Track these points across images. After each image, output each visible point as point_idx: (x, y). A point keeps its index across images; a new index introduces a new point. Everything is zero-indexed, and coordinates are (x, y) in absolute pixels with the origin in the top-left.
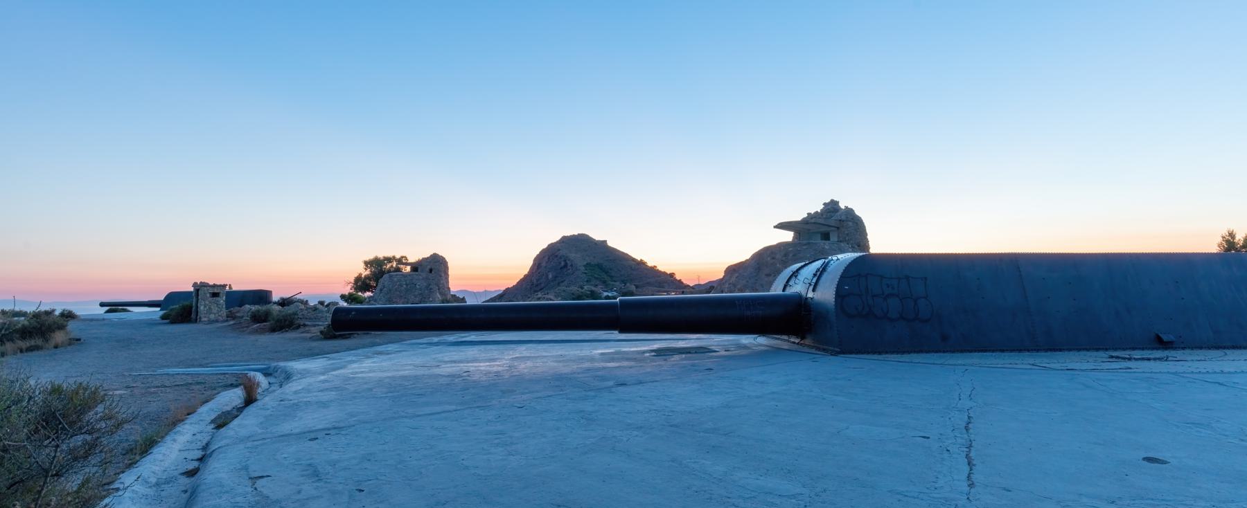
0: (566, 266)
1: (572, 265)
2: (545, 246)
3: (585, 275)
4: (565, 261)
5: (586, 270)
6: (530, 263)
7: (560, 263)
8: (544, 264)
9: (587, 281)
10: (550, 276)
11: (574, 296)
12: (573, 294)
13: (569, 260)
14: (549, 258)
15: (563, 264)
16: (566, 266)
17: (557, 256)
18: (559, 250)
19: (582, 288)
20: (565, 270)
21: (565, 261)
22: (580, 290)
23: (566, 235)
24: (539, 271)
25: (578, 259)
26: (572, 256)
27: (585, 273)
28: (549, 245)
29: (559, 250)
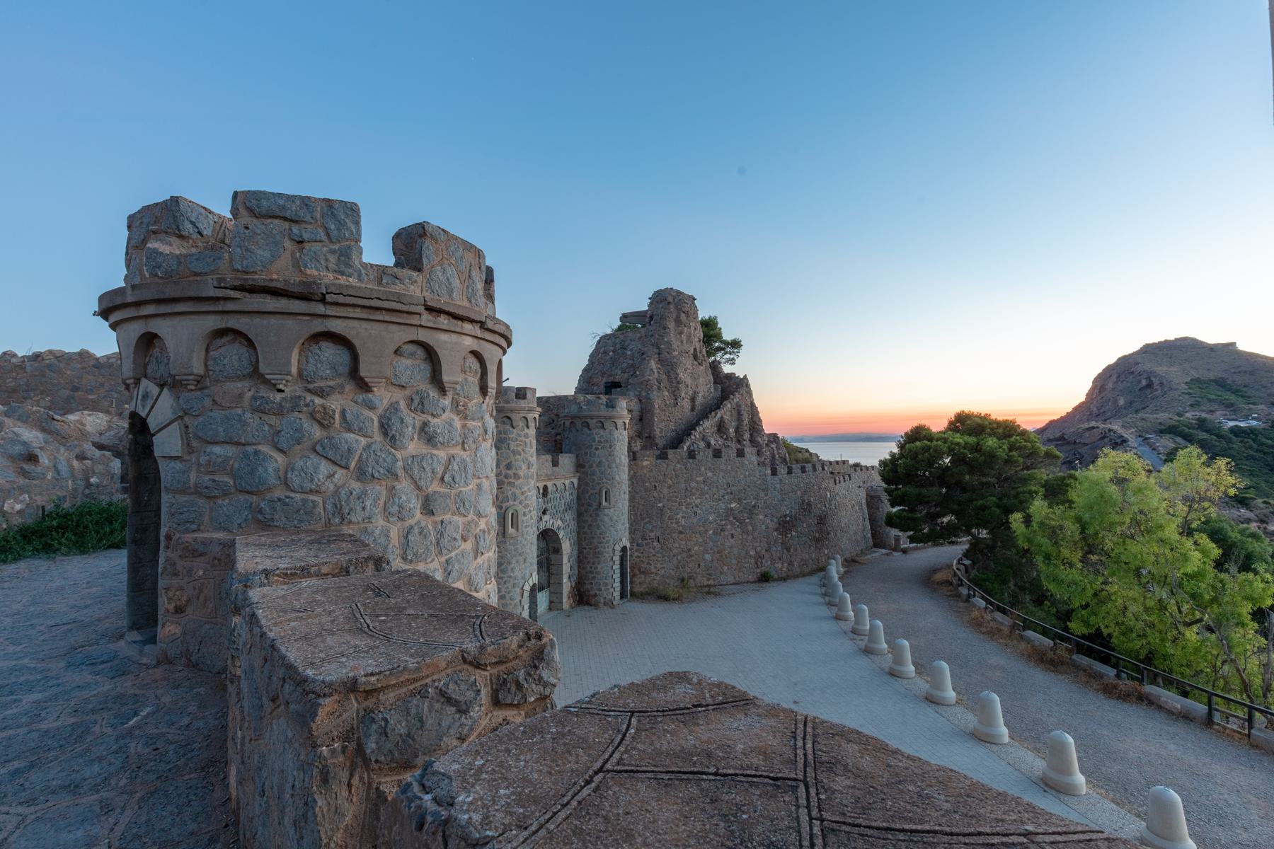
0: (1150, 385)
1: (1161, 384)
2: (1112, 360)
3: (1187, 397)
4: (1148, 378)
5: (1190, 388)
6: (1087, 385)
7: (1140, 382)
8: (1110, 385)
9: (1192, 405)
10: (1121, 402)
11: (1162, 427)
12: (1160, 424)
13: (1155, 377)
14: (1119, 377)
15: (1144, 382)
16: (1150, 385)
17: (1133, 373)
18: (1137, 364)
19: (1180, 415)
20: (1148, 391)
21: (1148, 378)
22: (1177, 418)
23: (1150, 341)
24: (1102, 395)
25: (1176, 375)
26: (1161, 370)
27: (1189, 394)
28: (1119, 359)
29: (1137, 364)
